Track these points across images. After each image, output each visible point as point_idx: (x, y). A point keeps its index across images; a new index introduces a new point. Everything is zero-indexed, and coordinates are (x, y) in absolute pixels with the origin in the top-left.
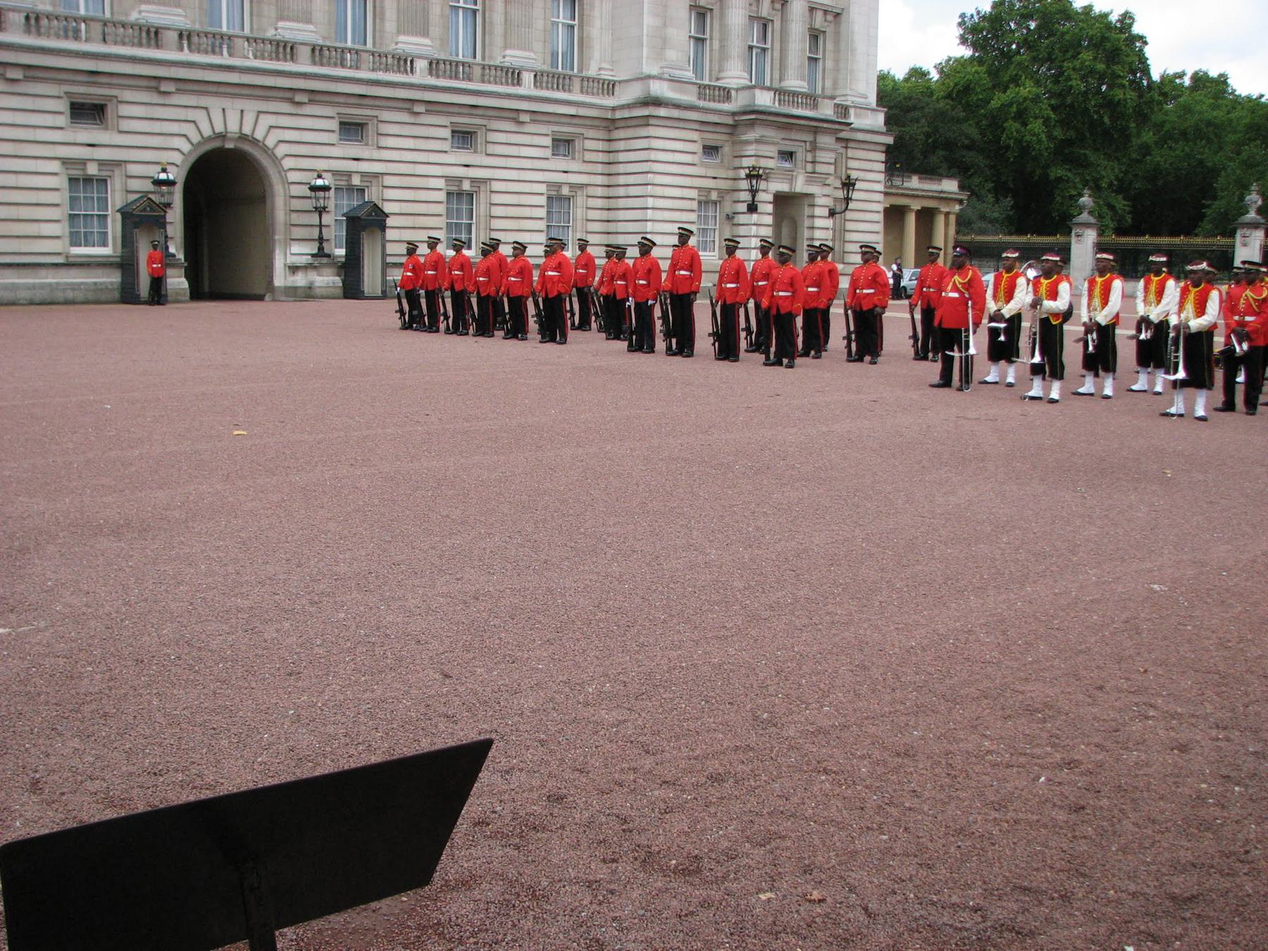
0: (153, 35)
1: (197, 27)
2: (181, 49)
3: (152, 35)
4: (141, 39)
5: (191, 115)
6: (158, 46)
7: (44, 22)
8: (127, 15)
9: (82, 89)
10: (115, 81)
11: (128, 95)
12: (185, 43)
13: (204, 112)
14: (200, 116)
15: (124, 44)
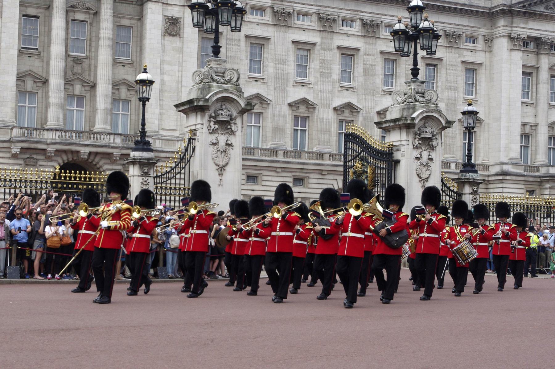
0: (320, 155)
1: (335, 152)
2: (330, 160)
3: (321, 156)
4: (317, 157)
5: (331, 182)
6: (322, 159)
7: (289, 153)
8: (313, 149)
9: (298, 174)
10: (308, 171)
11: (312, 176)
12: (331, 158)
13: (336, 181)
14: (334, 182)
15: (312, 159)
